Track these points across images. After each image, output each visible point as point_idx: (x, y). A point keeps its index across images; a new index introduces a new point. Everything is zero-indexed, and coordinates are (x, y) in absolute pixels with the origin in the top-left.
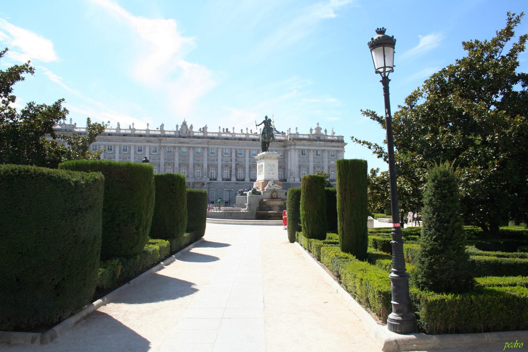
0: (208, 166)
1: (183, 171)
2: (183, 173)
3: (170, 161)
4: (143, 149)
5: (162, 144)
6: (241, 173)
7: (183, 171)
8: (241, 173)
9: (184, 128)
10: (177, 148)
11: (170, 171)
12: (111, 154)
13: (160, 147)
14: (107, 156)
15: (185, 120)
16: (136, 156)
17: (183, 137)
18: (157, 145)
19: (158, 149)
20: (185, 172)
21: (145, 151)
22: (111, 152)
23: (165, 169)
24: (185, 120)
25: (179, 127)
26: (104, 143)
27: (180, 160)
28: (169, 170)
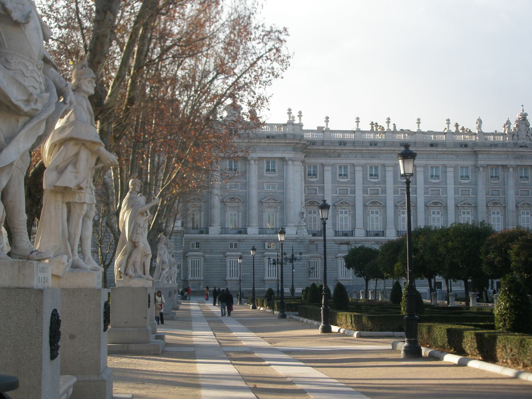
0: (516, 206)
1: (523, 218)
2: (524, 222)
3: (497, 197)
4: (442, 172)
5: (480, 163)
6: (528, 218)
7: (523, 218)
8: (498, 218)
9: (523, 127)
10: (511, 170)
11: (468, 218)
12: (375, 183)
13: (476, 167)
14: (369, 189)
15: (523, 111)
16: (428, 188)
17: (521, 147)
18: (470, 163)
19: (472, 172)
20: (528, 218)
21: (446, 177)
22: (376, 180)
23: (487, 213)
24: (523, 111)
25: (513, 126)
26: (363, 162)
27: (517, 194)
28: (466, 216)
